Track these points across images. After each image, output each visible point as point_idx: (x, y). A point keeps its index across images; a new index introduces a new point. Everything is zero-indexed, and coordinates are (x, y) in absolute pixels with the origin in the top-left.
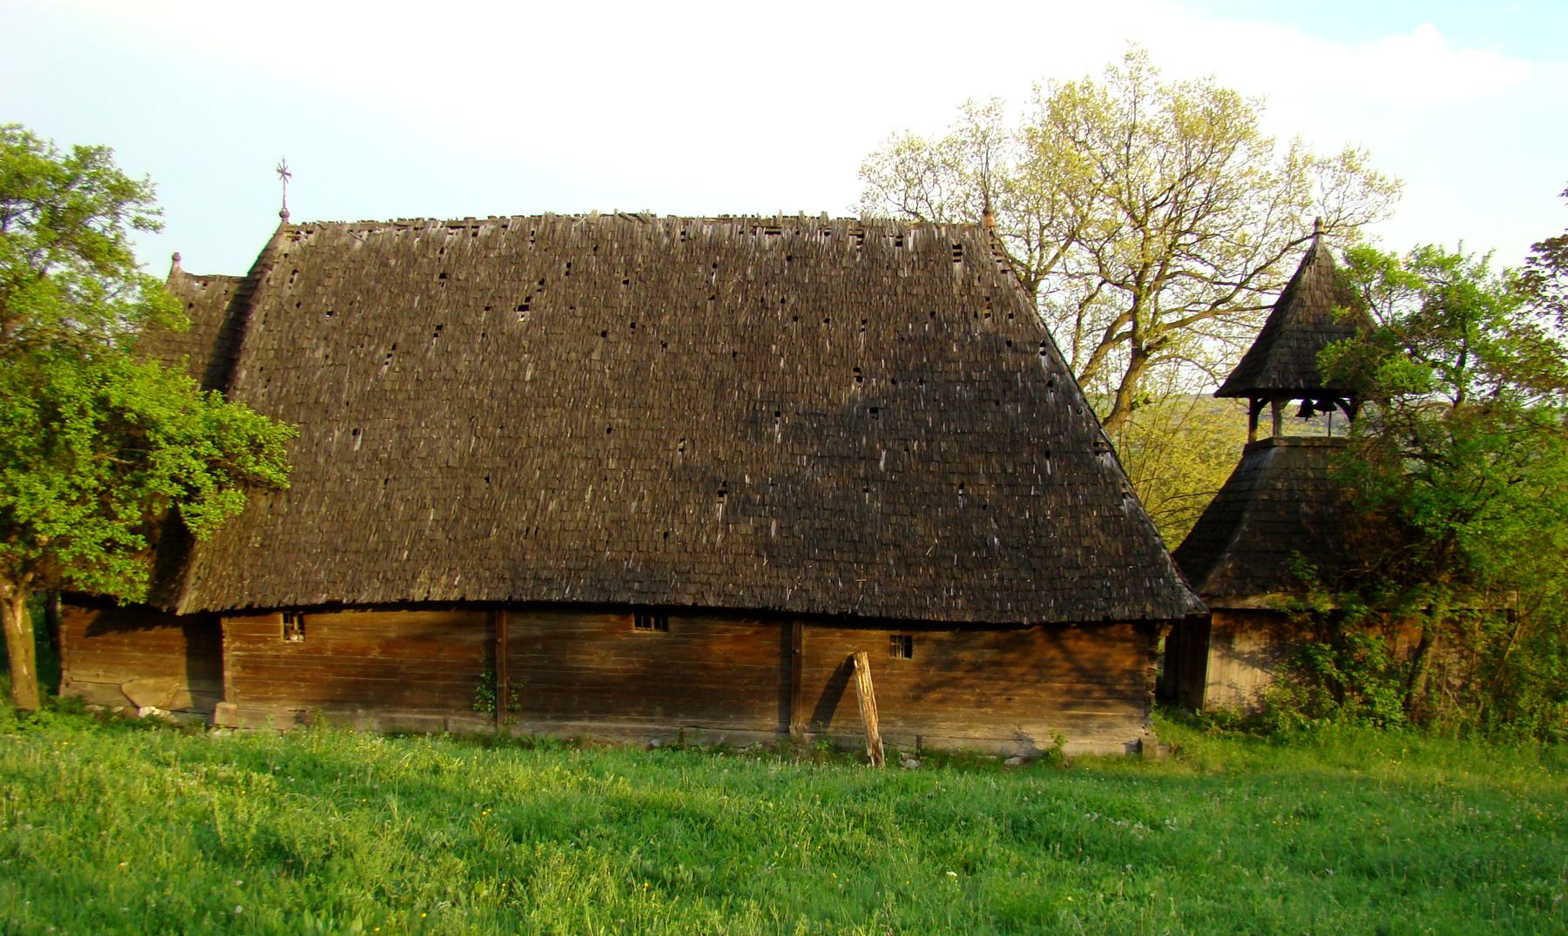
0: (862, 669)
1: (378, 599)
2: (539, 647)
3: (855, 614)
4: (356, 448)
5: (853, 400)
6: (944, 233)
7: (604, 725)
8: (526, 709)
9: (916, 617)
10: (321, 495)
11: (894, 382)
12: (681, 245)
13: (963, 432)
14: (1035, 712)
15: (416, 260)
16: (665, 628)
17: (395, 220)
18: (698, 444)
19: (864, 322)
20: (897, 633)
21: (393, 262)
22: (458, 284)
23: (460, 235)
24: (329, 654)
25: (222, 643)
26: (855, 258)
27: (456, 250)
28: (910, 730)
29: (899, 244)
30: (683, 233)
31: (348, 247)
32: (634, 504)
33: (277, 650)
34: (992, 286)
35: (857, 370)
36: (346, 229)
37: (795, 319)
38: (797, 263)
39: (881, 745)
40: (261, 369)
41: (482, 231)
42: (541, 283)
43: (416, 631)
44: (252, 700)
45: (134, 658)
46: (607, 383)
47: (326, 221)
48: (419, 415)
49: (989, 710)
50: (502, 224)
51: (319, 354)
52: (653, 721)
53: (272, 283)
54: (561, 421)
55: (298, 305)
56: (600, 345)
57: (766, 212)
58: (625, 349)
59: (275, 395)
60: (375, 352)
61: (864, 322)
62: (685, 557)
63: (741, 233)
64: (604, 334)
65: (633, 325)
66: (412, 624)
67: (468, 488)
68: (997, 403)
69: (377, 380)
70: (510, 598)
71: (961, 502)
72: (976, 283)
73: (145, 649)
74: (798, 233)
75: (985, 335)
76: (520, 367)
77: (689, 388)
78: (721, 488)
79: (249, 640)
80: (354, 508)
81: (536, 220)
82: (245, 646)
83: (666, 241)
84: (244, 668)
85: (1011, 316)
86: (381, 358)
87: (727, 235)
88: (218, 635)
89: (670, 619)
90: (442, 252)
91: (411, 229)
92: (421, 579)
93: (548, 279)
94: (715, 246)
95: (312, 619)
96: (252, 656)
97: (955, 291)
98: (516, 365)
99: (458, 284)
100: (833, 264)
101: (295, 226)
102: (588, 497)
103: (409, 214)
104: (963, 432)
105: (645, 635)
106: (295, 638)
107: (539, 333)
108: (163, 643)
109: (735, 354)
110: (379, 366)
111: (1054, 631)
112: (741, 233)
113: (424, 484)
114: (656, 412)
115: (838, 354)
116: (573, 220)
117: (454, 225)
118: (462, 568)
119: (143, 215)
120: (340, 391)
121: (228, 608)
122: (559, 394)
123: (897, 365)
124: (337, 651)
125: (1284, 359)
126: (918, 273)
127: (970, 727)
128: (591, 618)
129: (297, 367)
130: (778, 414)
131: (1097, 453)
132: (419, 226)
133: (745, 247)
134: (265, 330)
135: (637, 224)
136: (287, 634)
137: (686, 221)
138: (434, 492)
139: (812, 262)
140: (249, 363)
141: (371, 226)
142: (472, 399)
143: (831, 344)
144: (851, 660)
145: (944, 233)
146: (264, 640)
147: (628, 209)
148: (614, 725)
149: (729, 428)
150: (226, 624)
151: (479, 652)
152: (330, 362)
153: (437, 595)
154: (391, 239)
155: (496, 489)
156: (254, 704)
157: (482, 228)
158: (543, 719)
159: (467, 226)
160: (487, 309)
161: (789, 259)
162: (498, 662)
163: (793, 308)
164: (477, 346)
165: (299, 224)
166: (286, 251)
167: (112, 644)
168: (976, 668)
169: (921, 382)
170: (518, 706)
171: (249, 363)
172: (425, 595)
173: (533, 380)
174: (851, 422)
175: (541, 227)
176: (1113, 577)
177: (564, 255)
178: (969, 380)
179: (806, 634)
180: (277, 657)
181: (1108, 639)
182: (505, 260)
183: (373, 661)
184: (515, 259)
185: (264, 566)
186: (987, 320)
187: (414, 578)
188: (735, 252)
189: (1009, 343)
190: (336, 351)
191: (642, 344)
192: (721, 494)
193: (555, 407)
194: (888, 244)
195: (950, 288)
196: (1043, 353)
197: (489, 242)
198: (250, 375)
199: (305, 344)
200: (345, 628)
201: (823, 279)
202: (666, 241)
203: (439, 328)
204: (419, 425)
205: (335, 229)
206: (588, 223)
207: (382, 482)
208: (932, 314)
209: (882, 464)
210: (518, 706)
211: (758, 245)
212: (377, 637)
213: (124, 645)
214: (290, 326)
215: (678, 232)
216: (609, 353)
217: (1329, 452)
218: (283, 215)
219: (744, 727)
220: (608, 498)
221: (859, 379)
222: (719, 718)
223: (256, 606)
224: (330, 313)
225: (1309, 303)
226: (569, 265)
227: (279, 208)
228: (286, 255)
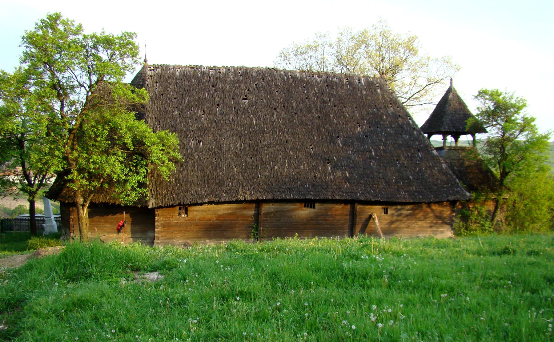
1: (227, 200)
2: (272, 215)
3: (380, 200)
9: (397, 201)
11: (370, 127)
12: (291, 80)
14: (422, 229)
15: (201, 80)
19: (356, 108)
22: (219, 90)
25: (155, 218)
29: (359, 83)
30: (291, 75)
32: (302, 166)
35: (358, 123)
36: (171, 67)
37: (335, 106)
40: (155, 118)
42: (248, 90)
43: (230, 211)
45: (106, 227)
46: (282, 126)
49: (409, 230)
51: (177, 113)
56: (275, 113)
58: (284, 114)
62: (323, 184)
64: (275, 109)
65: (284, 106)
66: (231, 209)
67: (246, 161)
68: (401, 135)
69: (201, 123)
71: (399, 165)
75: (392, 113)
76: (251, 119)
78: (327, 161)
82: (164, 219)
83: (286, 78)
85: (398, 107)
86: (200, 115)
87: (305, 76)
88: (154, 215)
89: (316, 204)
90: (210, 78)
94: (302, 80)
95: (191, 209)
96: (166, 223)
98: (249, 119)
99: (219, 90)
100: (341, 88)
102: (287, 164)
106: (183, 216)
110: (201, 118)
111: (429, 204)
114: (300, 136)
117: (210, 69)
125: (449, 122)
128: (290, 204)
129: (170, 118)
130: (338, 137)
131: (432, 150)
132: (197, 68)
133: (312, 81)
134: (152, 103)
135: (275, 72)
136: (180, 214)
139: (335, 87)
140: (150, 115)
142: (237, 130)
144: (371, 216)
151: (252, 218)
153: (248, 197)
154: (190, 72)
155: (255, 161)
159: (228, 69)
160: (233, 99)
161: (327, 86)
162: (260, 221)
165: (152, 64)
166: (151, 74)
167: (96, 222)
168: (407, 216)
169: (378, 128)
172: (244, 198)
173: (256, 125)
174: (362, 141)
176: (446, 188)
177: (254, 81)
178: (391, 127)
179: (359, 207)
180: (177, 223)
182: (233, 82)
185: (179, 189)
186: (391, 108)
189: (400, 116)
190: (182, 112)
193: (267, 134)
197: (226, 75)
199: (170, 109)
200: (203, 211)
203: (218, 105)
204: (222, 139)
205: (168, 67)
206: (258, 71)
207: (214, 159)
208: (376, 106)
209: (373, 153)
210: (265, 236)
211: (316, 81)
212: (215, 214)
213: (101, 222)
214: (162, 102)
216: (279, 115)
217: (459, 151)
220: (293, 164)
221: (360, 126)
224: (175, 98)
225: (452, 105)
226: (256, 85)
228: (151, 76)
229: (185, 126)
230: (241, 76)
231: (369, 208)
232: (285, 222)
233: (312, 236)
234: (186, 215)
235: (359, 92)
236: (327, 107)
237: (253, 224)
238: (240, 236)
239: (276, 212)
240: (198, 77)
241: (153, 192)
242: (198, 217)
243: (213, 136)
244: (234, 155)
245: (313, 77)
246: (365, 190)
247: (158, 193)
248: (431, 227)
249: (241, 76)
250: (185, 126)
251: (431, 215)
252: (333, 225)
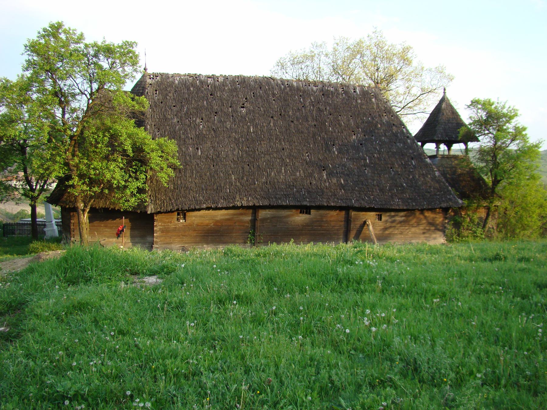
1: (225, 206)
3: (374, 207)
9: (391, 208)
11: (364, 136)
12: (288, 88)
13: (388, 152)
15: (200, 89)
19: (351, 116)
20: (378, 213)
25: (154, 223)
27: (213, 86)
29: (355, 92)
30: (287, 84)
32: (298, 173)
33: (175, 226)
35: (353, 132)
36: (170, 76)
40: (155, 125)
42: (246, 99)
43: (227, 217)
45: (106, 231)
46: (278, 133)
51: (175, 120)
58: (280, 123)
64: (272, 117)
65: (280, 115)
66: (228, 214)
67: (243, 168)
68: (395, 143)
70: (270, 204)
71: (393, 173)
76: (248, 127)
77: (304, 136)
78: (323, 168)
82: (163, 224)
83: (283, 87)
85: (392, 116)
86: (199, 123)
87: (301, 85)
88: (153, 220)
89: (311, 210)
90: (208, 86)
94: (298, 89)
96: (165, 228)
98: (247, 127)
100: (337, 97)
102: (283, 171)
104: (388, 152)
106: (181, 221)
110: (199, 126)
111: (422, 211)
114: (296, 143)
117: (209, 77)
125: (442, 131)
128: (286, 211)
129: (169, 125)
130: (334, 145)
131: (425, 158)
132: (196, 77)
133: (308, 90)
134: (152, 111)
135: (272, 81)
139: (330, 96)
140: (149, 123)
142: (235, 138)
143: (343, 123)
144: (365, 222)
149: (320, 149)
151: (249, 223)
153: (245, 203)
155: (252, 168)
156: (165, 245)
159: (226, 78)
160: (230, 107)
161: (323, 95)
162: (256, 226)
165: (151, 73)
168: (400, 222)
169: (372, 136)
173: (253, 132)
174: (356, 149)
176: (439, 195)
177: (251, 90)
179: (353, 213)
180: (176, 228)
181: (435, 213)
182: (231, 91)
185: (177, 195)
186: (386, 117)
189: (394, 125)
190: (181, 120)
197: (224, 84)
199: (169, 117)
200: (201, 216)
203: (216, 113)
204: (220, 146)
207: (212, 166)
208: (370, 114)
209: (368, 161)
210: (262, 241)
211: (312, 90)
213: (102, 227)
214: (161, 110)
216: (276, 123)
220: (290, 171)
221: (355, 135)
224: (174, 106)
225: (445, 114)
226: (253, 93)
228: (151, 84)
229: (184, 134)
230: (239, 84)
231: (363, 215)
232: (281, 228)
235: (355, 101)
236: (322, 115)
237: (250, 229)
238: (237, 241)
239: (273, 218)
240: (197, 85)
241: (152, 198)
242: (196, 222)
243: (211, 144)
244: (231, 161)
245: (310, 86)
246: (360, 197)
247: (157, 199)
248: (424, 233)
249: (239, 84)
250: (184, 134)
251: (424, 221)
252: (327, 231)
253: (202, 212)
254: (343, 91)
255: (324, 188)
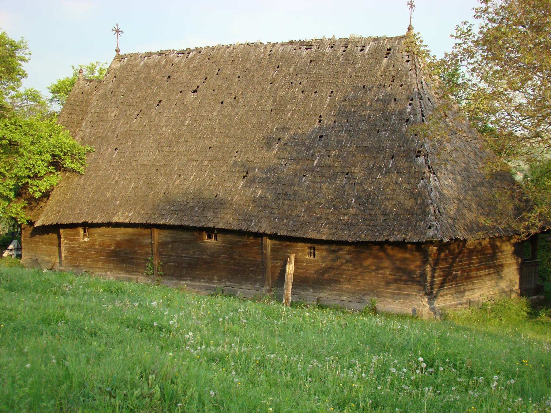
0: (290, 262)
4: (114, 156)
5: (313, 132)
6: (385, 43)
7: (195, 283)
8: (165, 275)
10: (96, 176)
16: (217, 239)
17: (159, 51)
18: (242, 154)
20: (309, 245)
21: (152, 71)
23: (182, 57)
24: (97, 247)
26: (339, 59)
28: (316, 294)
29: (362, 50)
30: (271, 51)
31: (137, 65)
32: (209, 181)
33: (79, 244)
34: (398, 70)
36: (140, 56)
38: (313, 63)
39: (290, 299)
41: (191, 55)
44: (71, 266)
47: (133, 53)
48: (141, 141)
50: (199, 51)
52: (213, 283)
53: (105, 82)
54: (193, 144)
55: (112, 92)
57: (308, 37)
58: (228, 110)
59: (92, 133)
60: (133, 113)
61: (332, 92)
63: (295, 49)
65: (235, 98)
66: (125, 234)
72: (391, 68)
73: (46, 244)
74: (318, 48)
79: (71, 240)
80: (106, 183)
81: (213, 48)
82: (68, 242)
84: (68, 252)
87: (289, 50)
91: (164, 55)
92: (119, 213)
93: (208, 77)
95: (93, 230)
96: (70, 247)
97: (379, 74)
98: (184, 118)
101: (122, 56)
102: (192, 178)
103: (164, 49)
105: (209, 242)
106: (86, 239)
107: (197, 104)
108: (51, 241)
109: (272, 110)
112: (295, 49)
113: (133, 172)
115: (314, 109)
116: (228, 48)
117: (182, 52)
118: (135, 209)
119: (23, 55)
120: (115, 131)
121: (50, 224)
122: (196, 131)
123: (339, 113)
124: (100, 246)
126: (364, 65)
127: (341, 294)
137: (274, 45)
138: (136, 176)
140: (87, 119)
141: (149, 54)
145: (385, 43)
146: (74, 240)
147: (251, 41)
148: (198, 284)
150: (62, 231)
151: (149, 248)
152: (116, 118)
157: (191, 53)
158: (173, 279)
162: (154, 252)
163: (304, 87)
164: (171, 110)
166: (114, 68)
170: (161, 273)
171: (87, 119)
173: (188, 125)
175: (214, 51)
180: (79, 247)
182: (196, 69)
183: (112, 250)
184: (198, 68)
187: (117, 213)
188: (289, 60)
191: (235, 107)
192: (244, 177)
194: (357, 50)
195: (377, 71)
196: (410, 104)
198: (86, 125)
200: (102, 235)
201: (321, 72)
202: (262, 56)
203: (160, 101)
204: (139, 146)
213: (39, 242)
215: (269, 50)
218: (118, 51)
219: (248, 288)
222: (239, 283)
223: (59, 223)
227: (115, 47)
230: (209, 59)
231: (288, 246)
232: (185, 257)
233: (218, 280)
234: (88, 239)
238: (139, 270)
239: (174, 242)
249: (209, 59)
253: (103, 229)
254: (344, 51)
255: (229, 201)
